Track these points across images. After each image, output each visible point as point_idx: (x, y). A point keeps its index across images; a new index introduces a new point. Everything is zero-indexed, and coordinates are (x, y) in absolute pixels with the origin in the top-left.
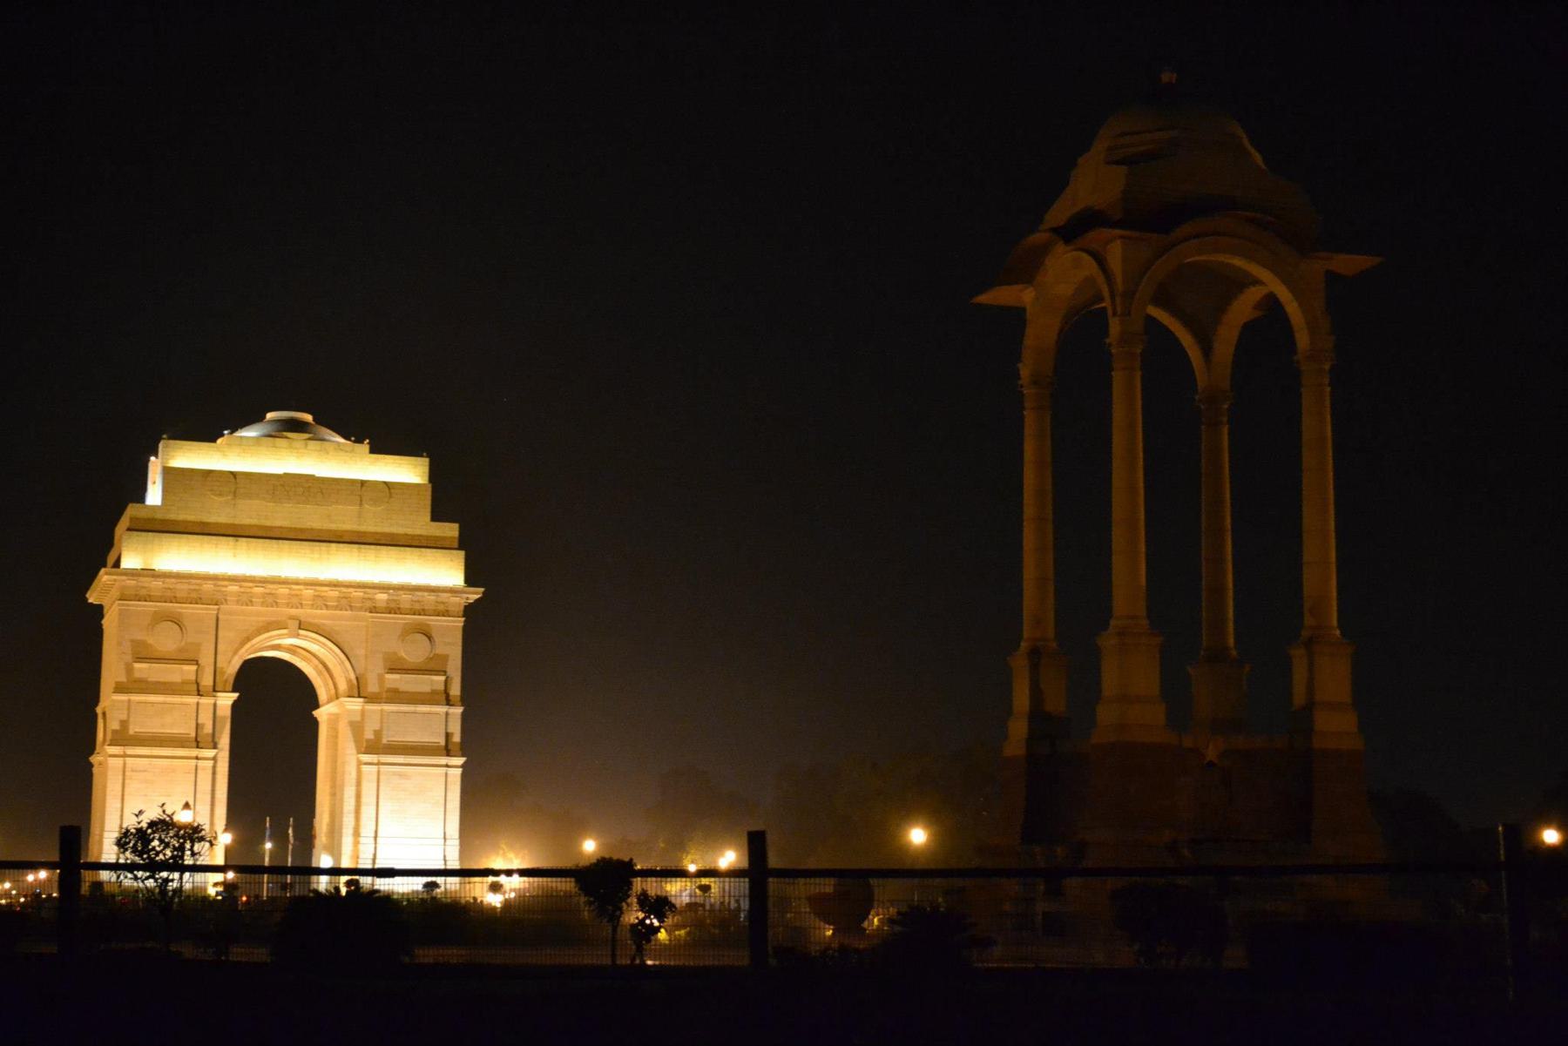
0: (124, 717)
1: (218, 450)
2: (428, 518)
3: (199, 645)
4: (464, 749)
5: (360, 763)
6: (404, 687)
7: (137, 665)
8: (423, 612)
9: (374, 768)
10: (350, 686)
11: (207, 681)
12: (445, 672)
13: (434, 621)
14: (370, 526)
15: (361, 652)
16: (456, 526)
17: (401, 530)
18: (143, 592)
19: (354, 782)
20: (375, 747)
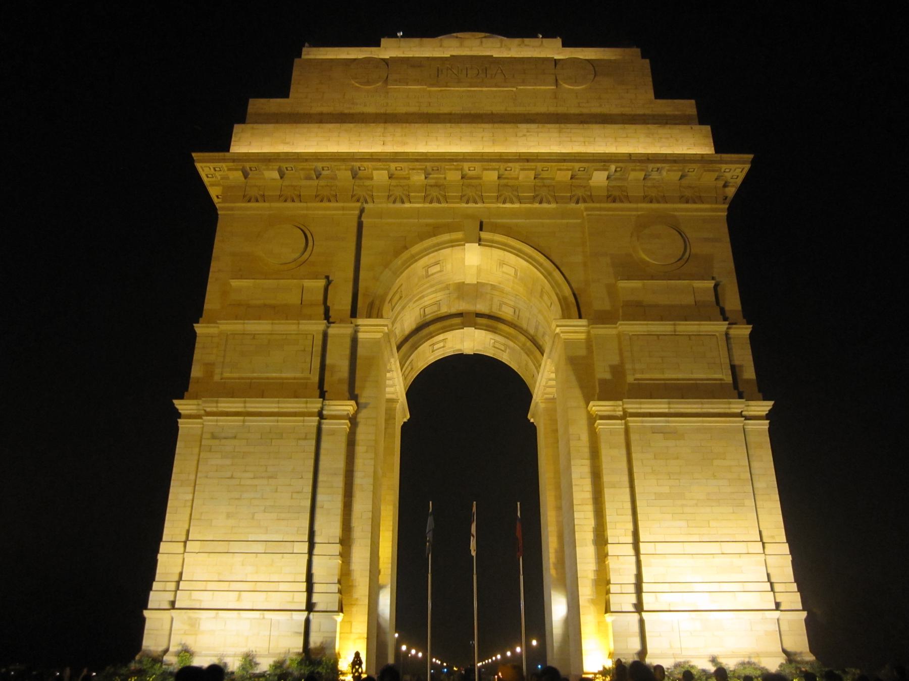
2: (651, 95)
5: (592, 419)
7: (235, 283)
8: (665, 199)
9: (619, 425)
11: (341, 301)
12: (713, 278)
16: (693, 102)
17: (615, 110)
18: (253, 192)
19: (586, 451)
20: (614, 388)
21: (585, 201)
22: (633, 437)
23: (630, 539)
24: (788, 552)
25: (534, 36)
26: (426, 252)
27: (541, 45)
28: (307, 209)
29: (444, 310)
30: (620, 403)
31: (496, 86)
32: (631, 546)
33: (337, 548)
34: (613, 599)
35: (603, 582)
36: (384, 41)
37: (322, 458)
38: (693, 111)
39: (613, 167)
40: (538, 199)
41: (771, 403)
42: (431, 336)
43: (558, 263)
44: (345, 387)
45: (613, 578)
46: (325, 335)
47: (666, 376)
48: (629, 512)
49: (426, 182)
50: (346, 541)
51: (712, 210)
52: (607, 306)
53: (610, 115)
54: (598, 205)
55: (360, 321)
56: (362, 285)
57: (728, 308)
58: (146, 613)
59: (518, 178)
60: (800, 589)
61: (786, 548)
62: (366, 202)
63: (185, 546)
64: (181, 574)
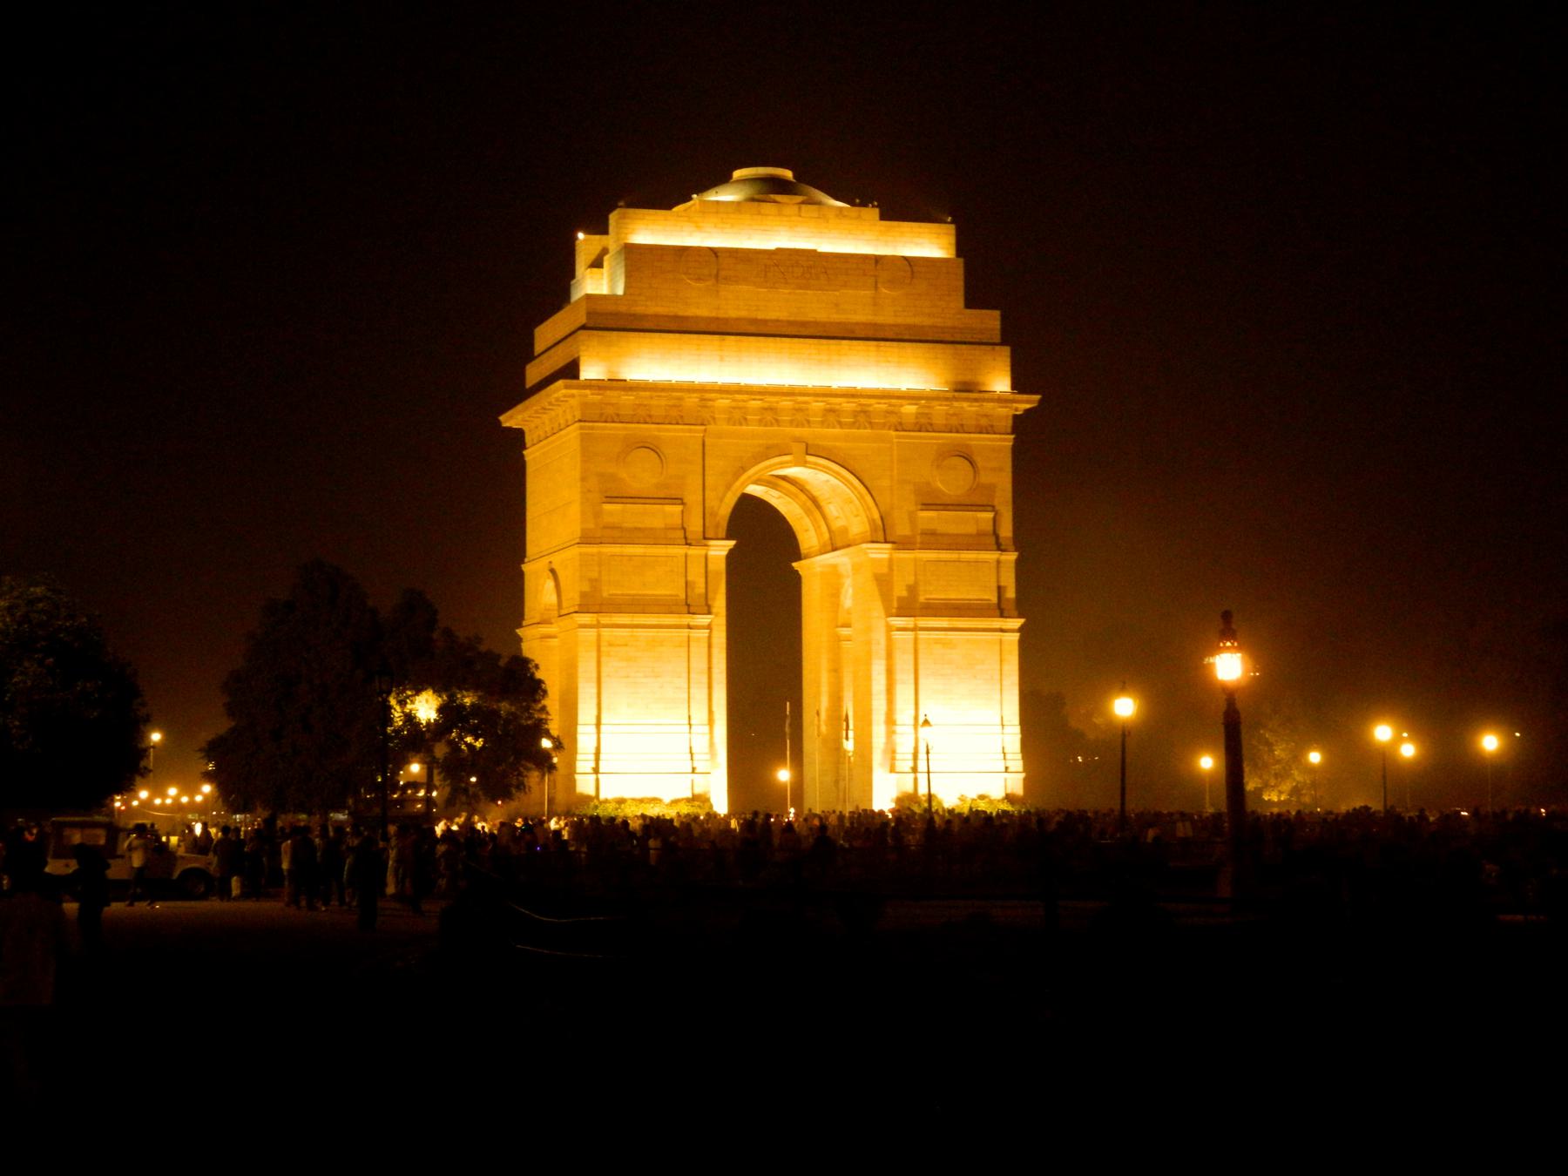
0: (595, 575)
1: (690, 219)
2: (961, 303)
5: (889, 629)
6: (941, 528)
7: (607, 507)
9: (910, 635)
10: (874, 529)
11: (695, 526)
12: (993, 508)
13: (976, 440)
14: (887, 317)
18: (610, 411)
19: (883, 653)
20: (910, 607)
22: (921, 647)
33: (707, 728)
34: (898, 764)
35: (891, 753)
41: (1022, 621)
44: (702, 601)
45: (899, 749)
50: (711, 722)
61: (1018, 729)
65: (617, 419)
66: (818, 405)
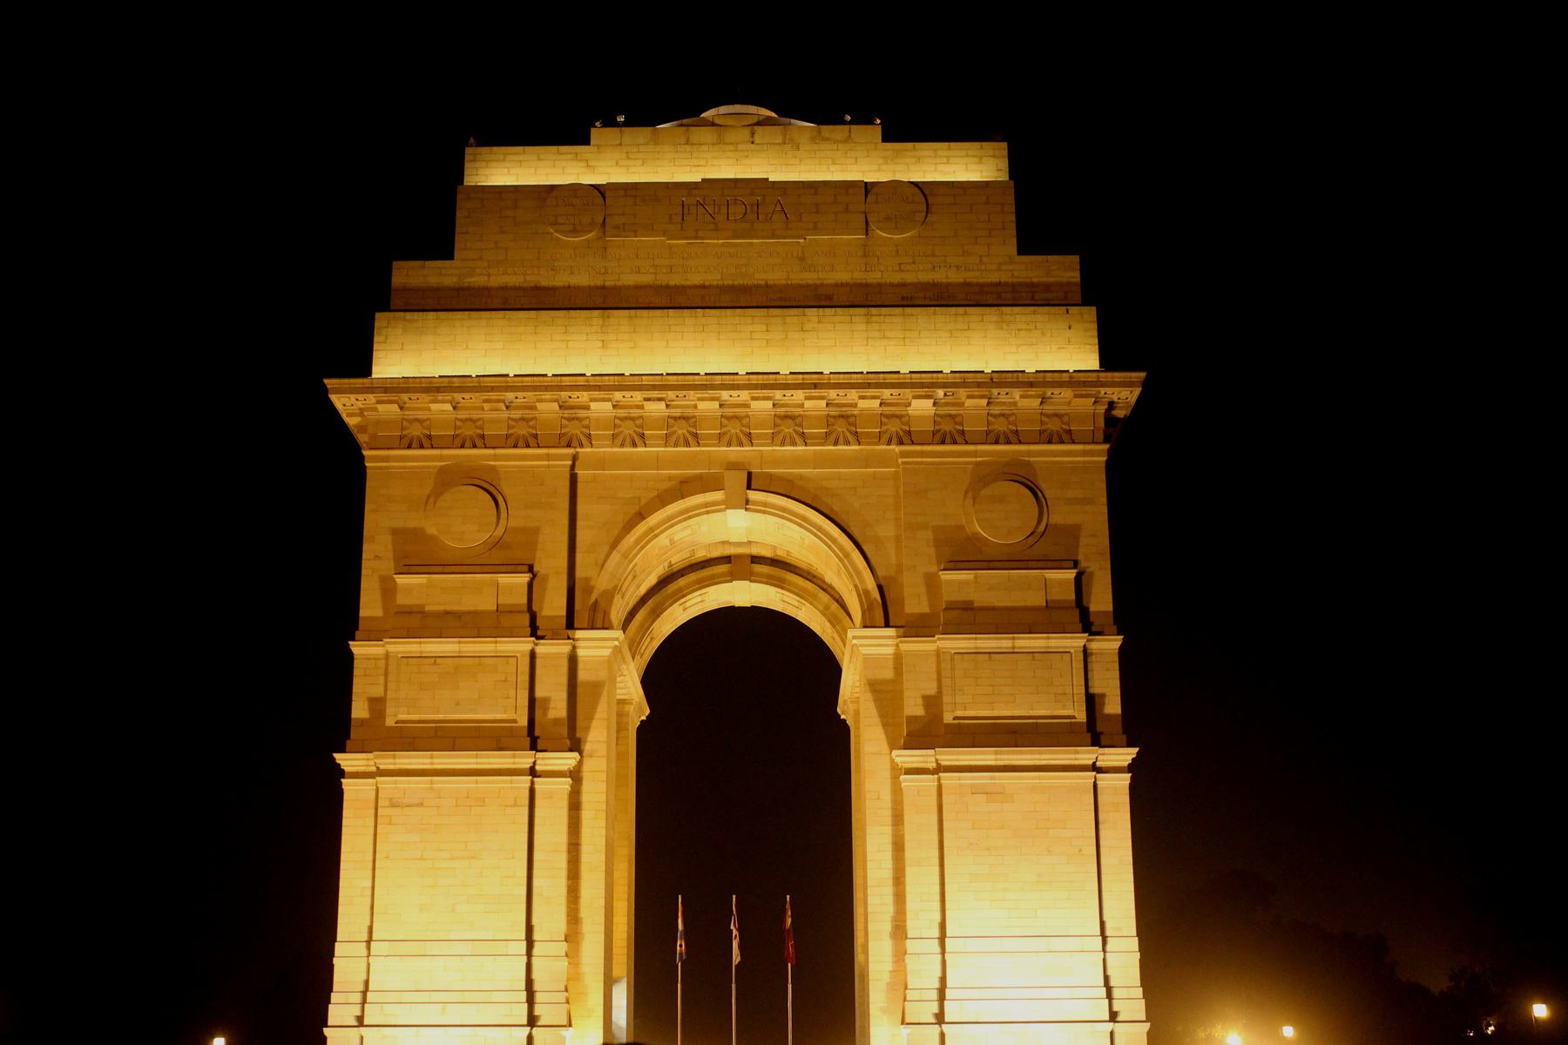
0: (378, 691)
2: (1012, 247)
3: (536, 531)
4: (1132, 729)
5: (897, 772)
6: (981, 598)
7: (402, 580)
9: (929, 781)
10: (867, 611)
11: (553, 605)
12: (1076, 564)
14: (886, 273)
15: (886, 531)
16: (1076, 259)
17: (955, 277)
18: (416, 431)
19: (887, 814)
20: (927, 732)
21: (901, 443)
23: (936, 933)
24: (1136, 947)
25: (837, 120)
26: (670, 522)
27: (848, 139)
28: (495, 458)
29: (701, 555)
30: (931, 752)
31: (774, 236)
32: (936, 942)
35: (900, 985)
36: (597, 134)
37: (537, 828)
38: (1074, 276)
39: (940, 393)
40: (832, 438)
42: (680, 594)
43: (860, 541)
44: (565, 732)
46: (533, 655)
47: (996, 713)
48: (938, 897)
49: (667, 412)
50: (573, 936)
51: (1085, 453)
52: (924, 608)
53: (948, 285)
54: (918, 448)
55: (579, 634)
56: (579, 573)
57: (1093, 608)
58: (326, 1031)
59: (802, 406)
60: (1145, 996)
61: (1134, 943)
62: (581, 445)
63: (369, 948)
64: (367, 983)
65: (426, 442)
66: (762, 407)
